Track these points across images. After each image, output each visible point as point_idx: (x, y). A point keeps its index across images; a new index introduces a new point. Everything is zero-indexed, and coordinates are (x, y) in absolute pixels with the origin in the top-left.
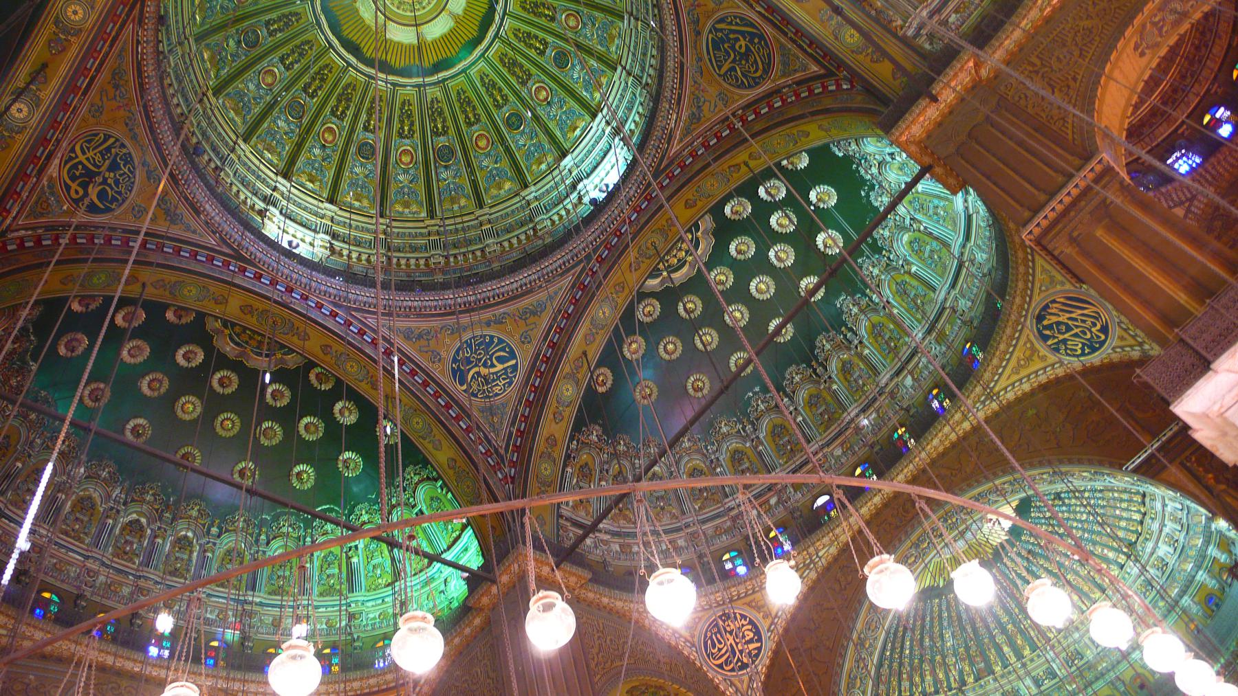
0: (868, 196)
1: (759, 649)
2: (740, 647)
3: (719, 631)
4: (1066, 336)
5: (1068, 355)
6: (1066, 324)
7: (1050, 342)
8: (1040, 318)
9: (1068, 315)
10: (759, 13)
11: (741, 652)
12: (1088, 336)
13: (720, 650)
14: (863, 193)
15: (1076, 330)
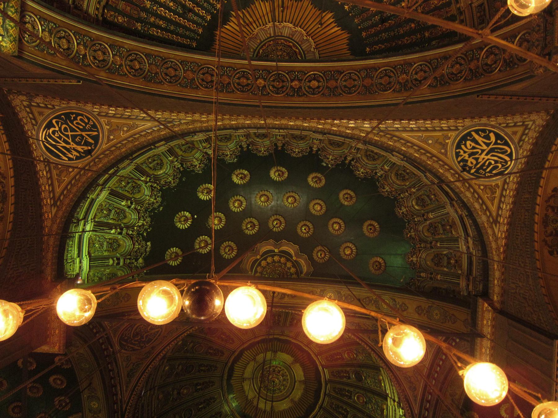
0: (159, 207)
1: (477, 132)
2: (485, 147)
3: (481, 167)
4: (79, 133)
5: (89, 119)
6: (73, 141)
7: (96, 133)
8: (89, 152)
9: (68, 146)
10: (112, 348)
11: (488, 145)
12: (64, 126)
13: (496, 162)
14: (161, 209)
15: (70, 133)
